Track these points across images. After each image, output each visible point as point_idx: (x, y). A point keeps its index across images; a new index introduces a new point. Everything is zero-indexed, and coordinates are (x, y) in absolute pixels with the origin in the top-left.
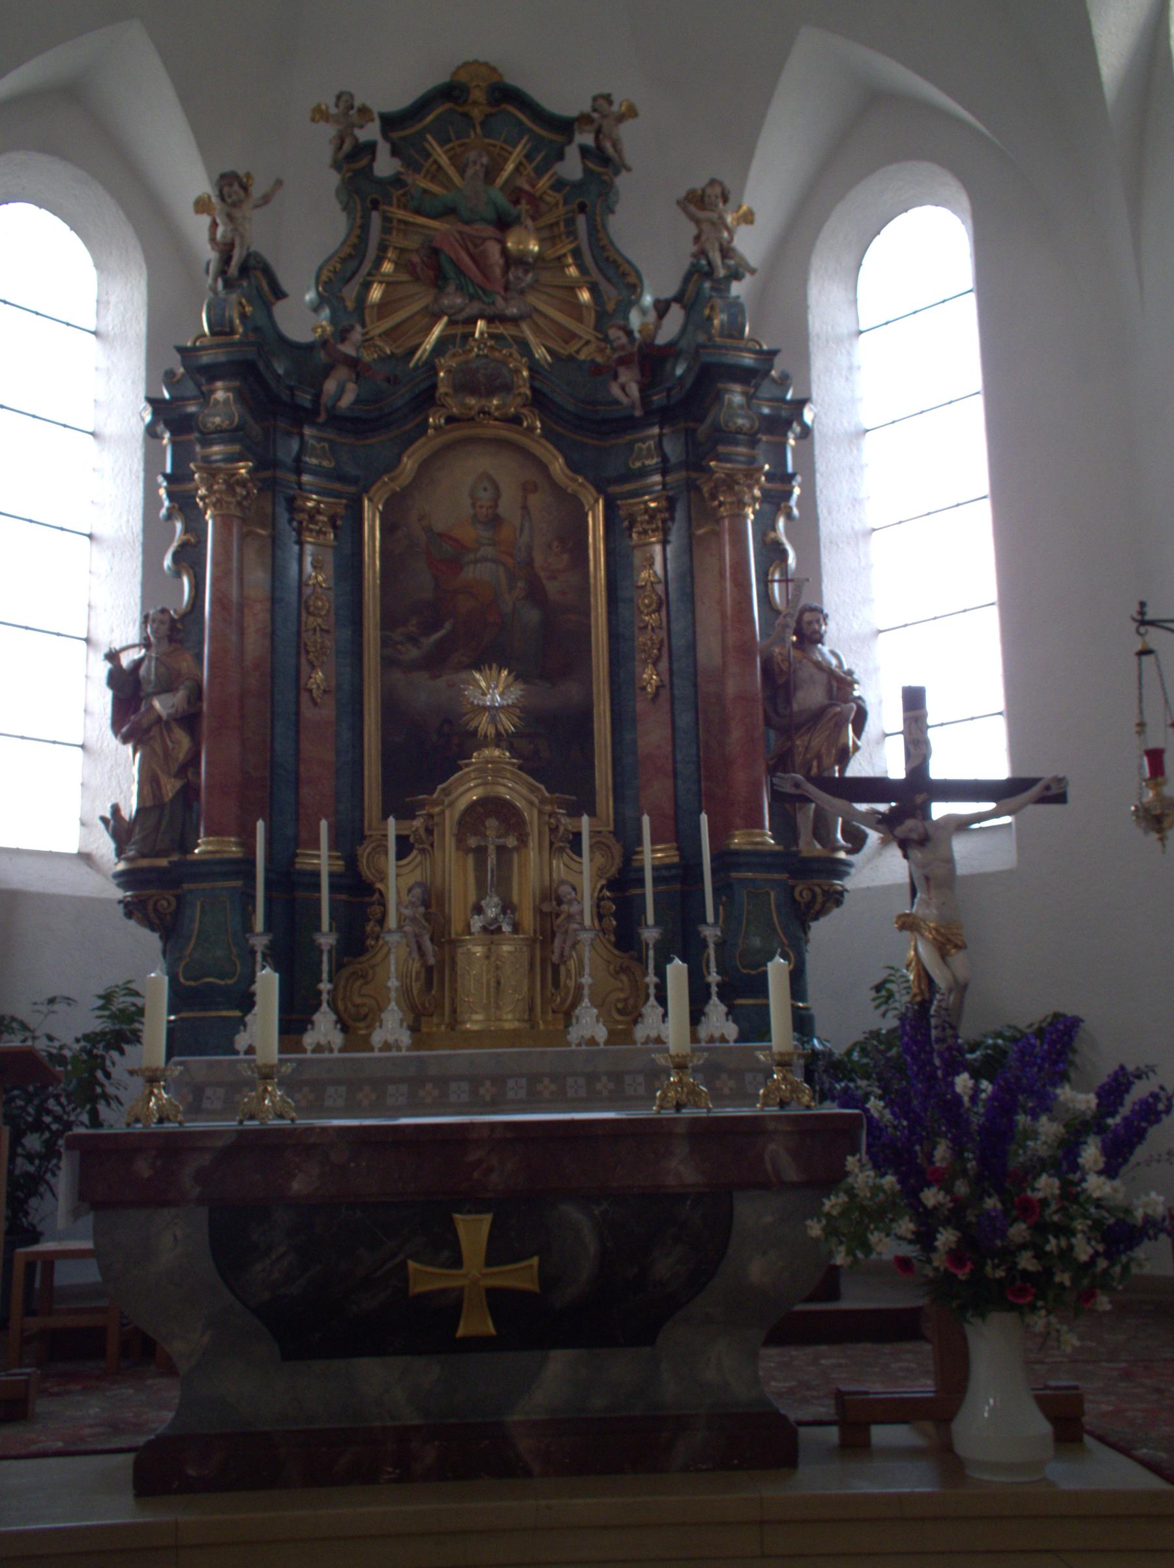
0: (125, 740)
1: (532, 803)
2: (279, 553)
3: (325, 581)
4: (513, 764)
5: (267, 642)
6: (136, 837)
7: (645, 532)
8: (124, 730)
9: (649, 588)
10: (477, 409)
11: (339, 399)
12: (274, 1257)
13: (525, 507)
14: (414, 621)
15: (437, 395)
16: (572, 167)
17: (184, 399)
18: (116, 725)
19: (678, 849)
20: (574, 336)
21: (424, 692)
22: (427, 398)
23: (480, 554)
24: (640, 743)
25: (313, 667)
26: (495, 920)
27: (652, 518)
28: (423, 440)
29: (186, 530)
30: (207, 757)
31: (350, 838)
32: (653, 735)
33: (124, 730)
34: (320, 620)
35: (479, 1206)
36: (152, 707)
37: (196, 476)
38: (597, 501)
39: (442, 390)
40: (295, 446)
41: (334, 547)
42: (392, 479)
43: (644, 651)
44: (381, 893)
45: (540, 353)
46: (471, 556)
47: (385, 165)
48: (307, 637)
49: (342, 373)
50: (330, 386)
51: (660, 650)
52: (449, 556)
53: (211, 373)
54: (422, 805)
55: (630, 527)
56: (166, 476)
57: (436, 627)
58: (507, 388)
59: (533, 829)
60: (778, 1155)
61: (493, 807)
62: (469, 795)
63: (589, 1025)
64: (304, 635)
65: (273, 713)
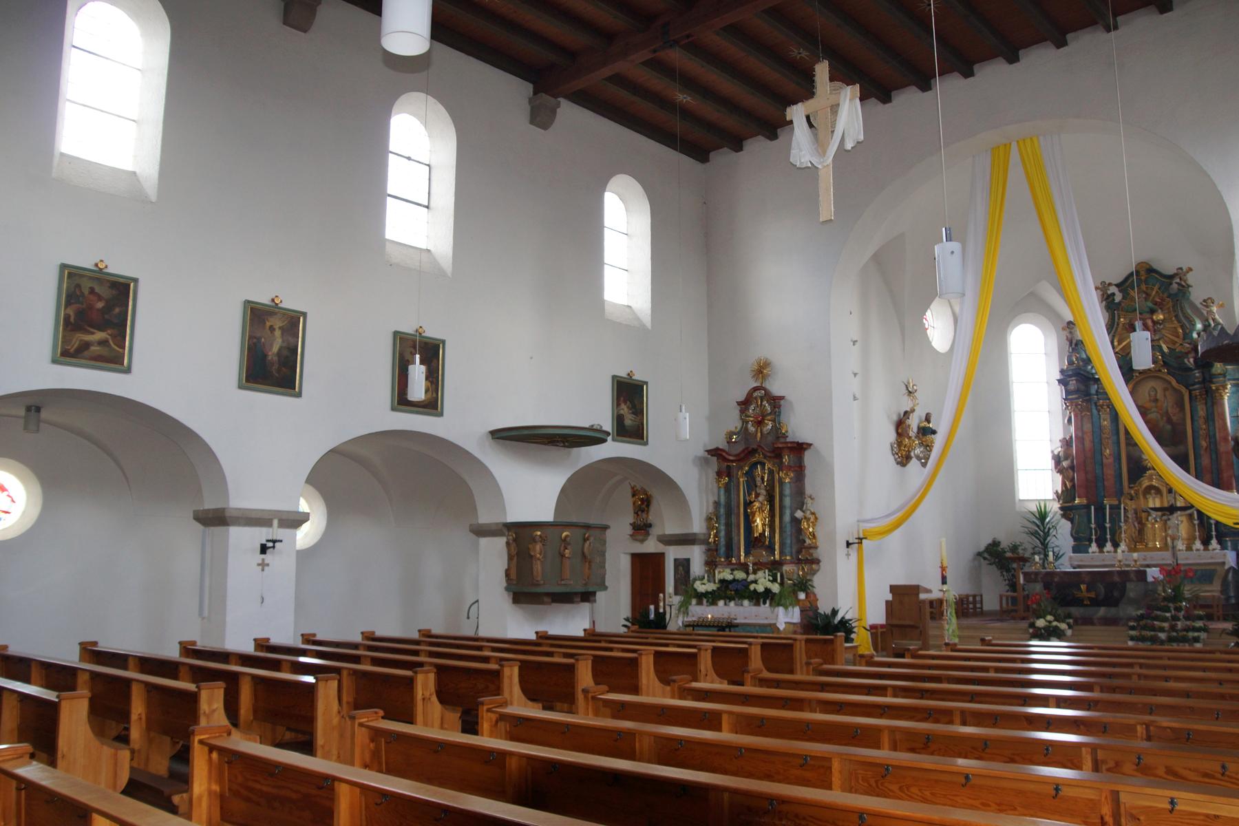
20: (1174, 343)
31: (1119, 493)
35: (1083, 583)
45: (1166, 350)
47: (1118, 297)
53: (1070, 376)
61: (1150, 488)
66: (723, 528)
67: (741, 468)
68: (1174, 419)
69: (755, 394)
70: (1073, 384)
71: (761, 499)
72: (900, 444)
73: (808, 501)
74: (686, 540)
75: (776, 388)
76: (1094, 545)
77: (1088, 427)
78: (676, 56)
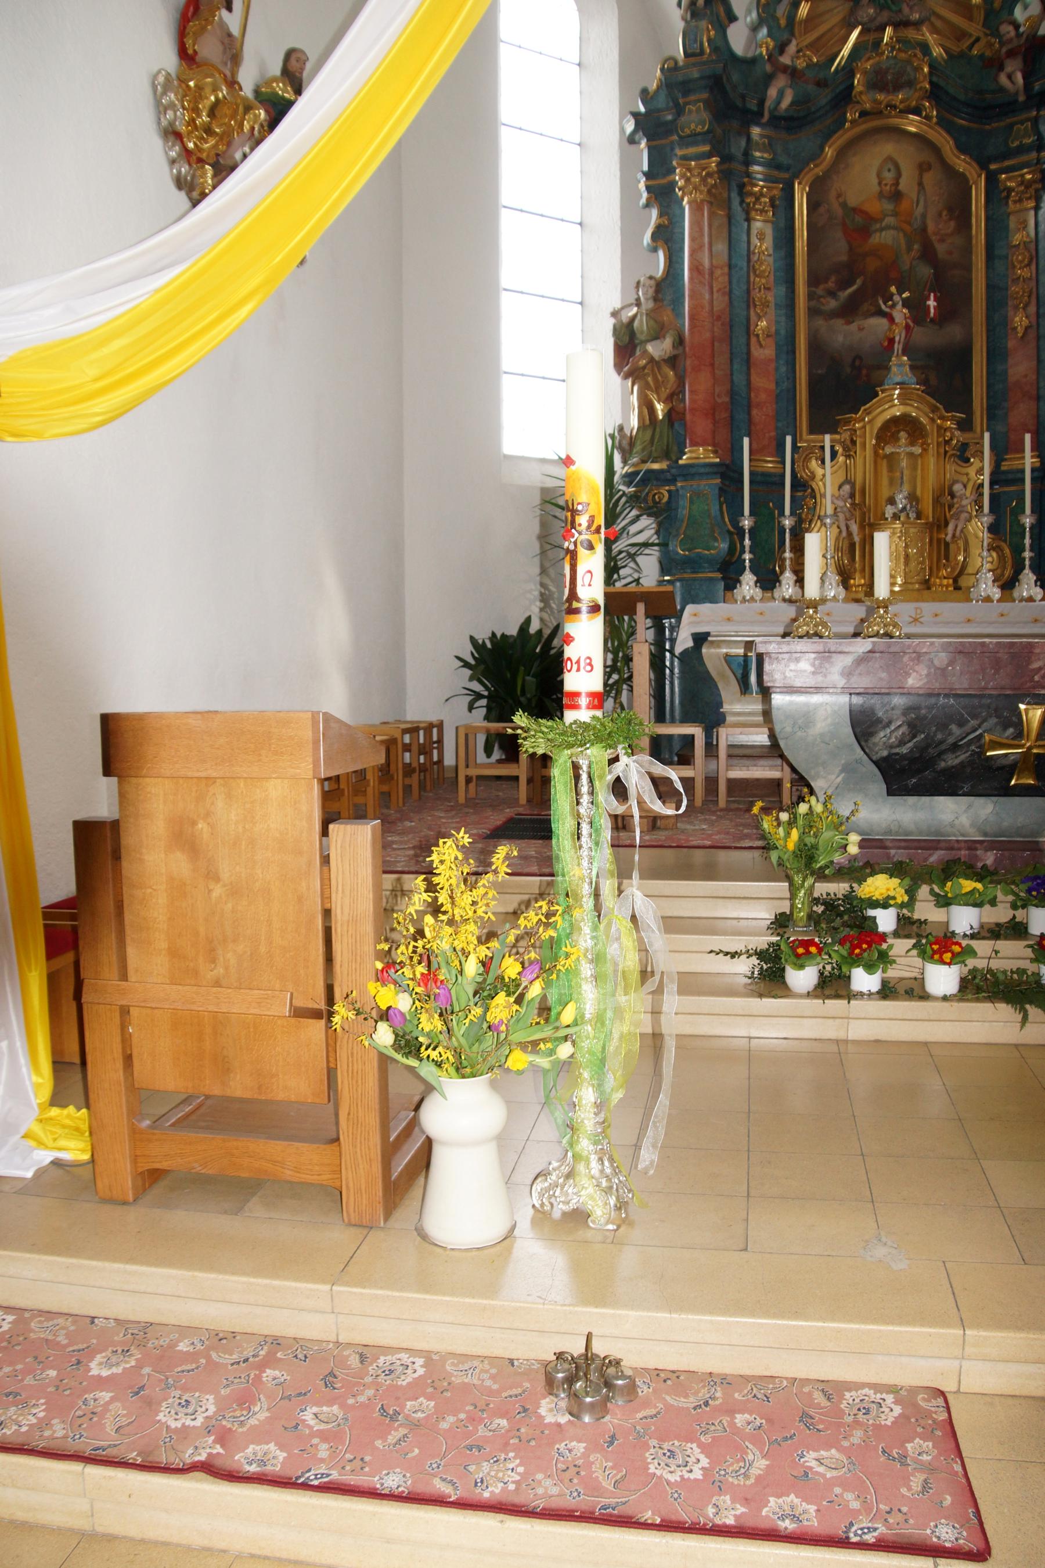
0: (626, 377)
1: (933, 420)
2: (734, 229)
3: (767, 249)
4: (918, 390)
5: (727, 298)
6: (638, 448)
7: (1020, 201)
8: (626, 369)
9: (1022, 246)
10: (884, 103)
11: (778, 102)
12: (893, 728)
13: (920, 184)
14: (833, 279)
15: (854, 93)
17: (659, 111)
18: (618, 366)
19: (1038, 457)
21: (843, 335)
22: (845, 96)
23: (884, 224)
24: (1011, 372)
25: (759, 318)
26: (904, 509)
27: (1027, 187)
28: (841, 132)
29: (661, 215)
30: (690, 386)
32: (1020, 367)
33: (626, 369)
34: (763, 281)
36: (645, 351)
37: (678, 171)
38: (980, 176)
40: (743, 143)
41: (772, 222)
42: (816, 166)
43: (1016, 298)
44: (813, 490)
46: (878, 226)
48: (756, 295)
49: (781, 81)
50: (772, 92)
51: (1029, 297)
52: (860, 225)
54: (847, 422)
55: (1008, 197)
56: (645, 174)
57: (849, 283)
59: (933, 439)
62: (885, 413)
64: (752, 293)
65: (731, 354)
68: (941, 249)
70: (696, 117)
76: (748, 579)
77: (721, 247)
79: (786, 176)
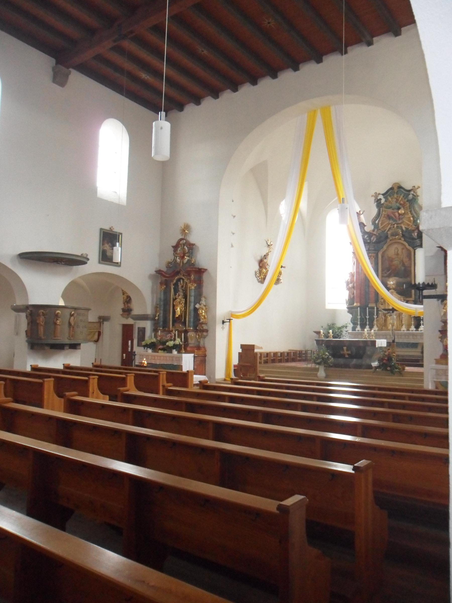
13: (402, 252)
16: (411, 196)
20: (409, 225)
22: (387, 237)
39: (389, 236)
45: (404, 229)
47: (383, 201)
50: (372, 238)
52: (391, 260)
57: (388, 271)
58: (398, 235)
60: (369, 343)
63: (404, 328)
66: (162, 312)
67: (172, 281)
68: (406, 264)
69: (181, 242)
71: (180, 297)
72: (260, 272)
73: (203, 299)
74: (144, 318)
75: (192, 239)
78: (128, 45)
79: (376, 252)
